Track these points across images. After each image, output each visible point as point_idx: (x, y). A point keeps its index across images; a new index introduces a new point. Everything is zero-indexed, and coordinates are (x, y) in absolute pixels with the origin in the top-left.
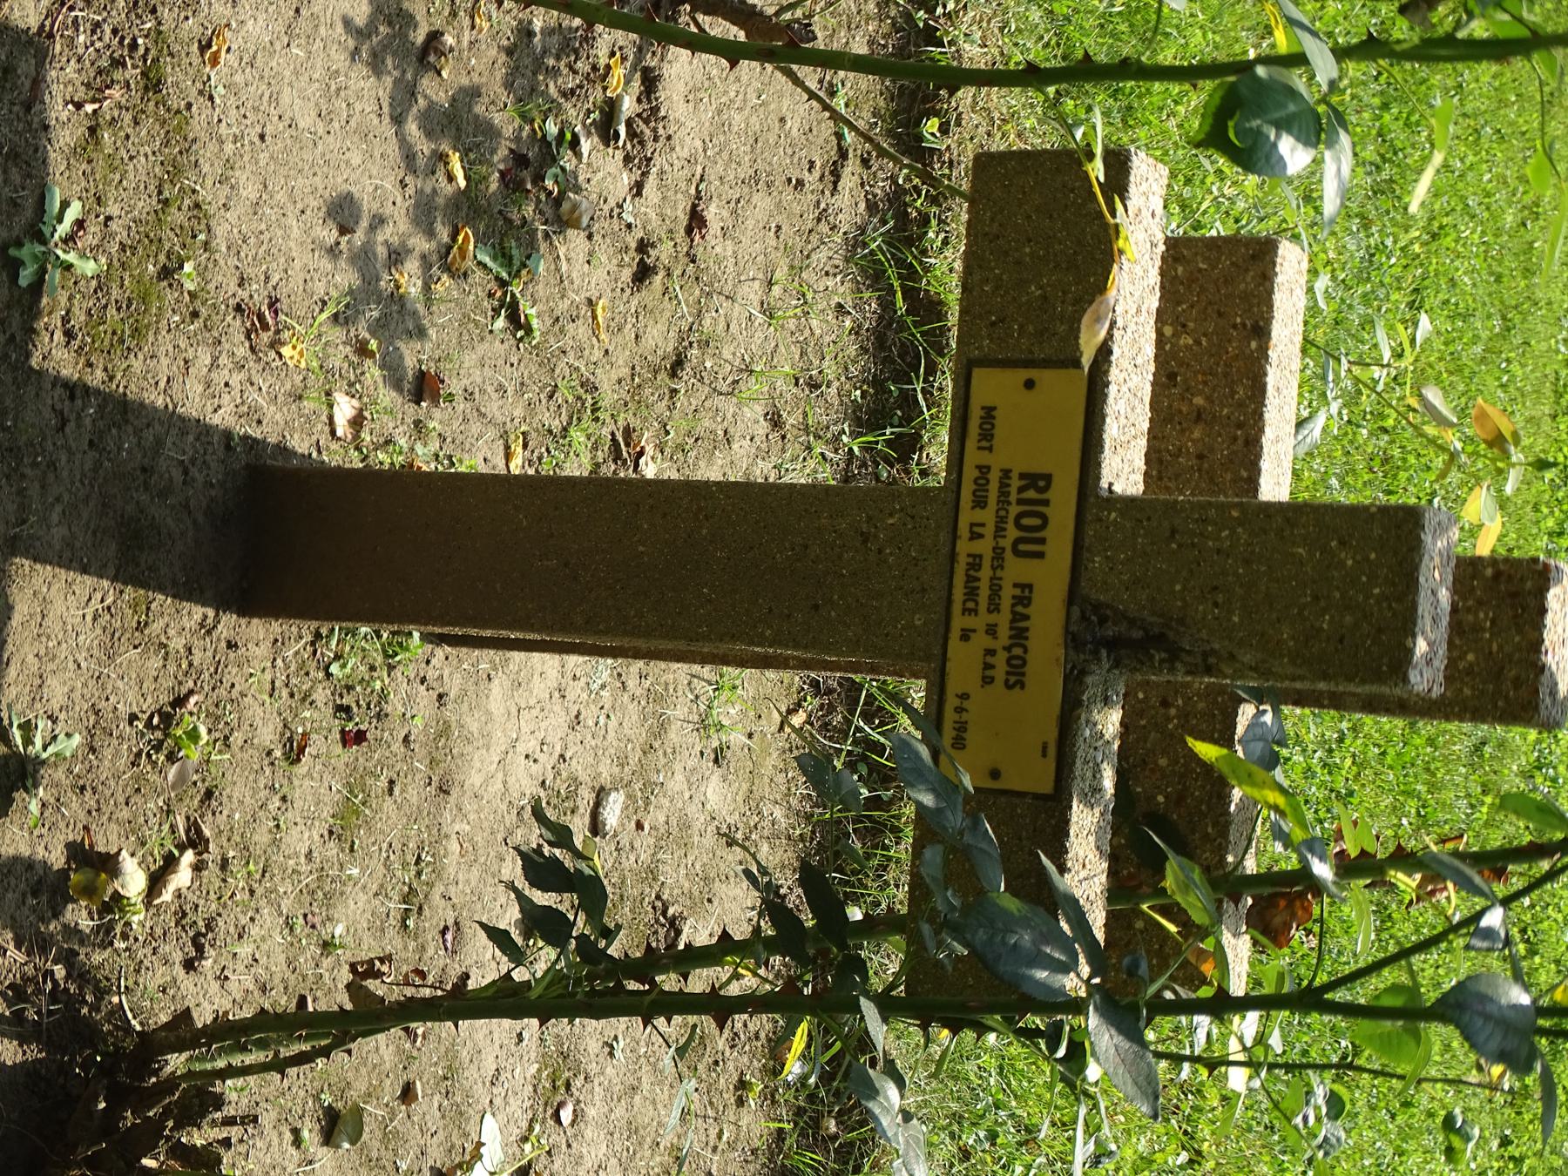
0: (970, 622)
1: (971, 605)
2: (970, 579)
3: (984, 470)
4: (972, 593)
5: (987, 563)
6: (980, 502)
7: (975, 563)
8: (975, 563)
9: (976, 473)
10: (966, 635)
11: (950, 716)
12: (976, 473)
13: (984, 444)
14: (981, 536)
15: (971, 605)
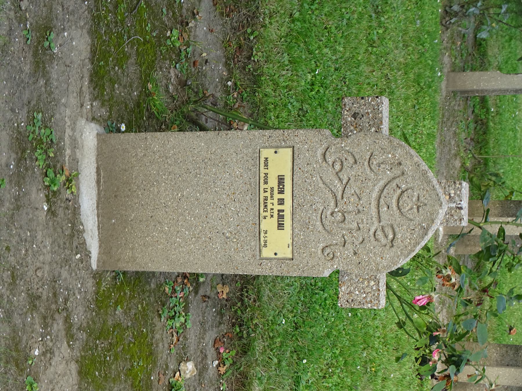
0: (265, 214)
1: (265, 210)
2: (265, 203)
3: (266, 174)
4: (266, 206)
5: (269, 198)
6: (266, 183)
7: (266, 199)
8: (266, 199)
9: (264, 175)
10: (265, 218)
11: (262, 239)
12: (264, 175)
13: (266, 167)
14: (267, 191)
15: (265, 210)
